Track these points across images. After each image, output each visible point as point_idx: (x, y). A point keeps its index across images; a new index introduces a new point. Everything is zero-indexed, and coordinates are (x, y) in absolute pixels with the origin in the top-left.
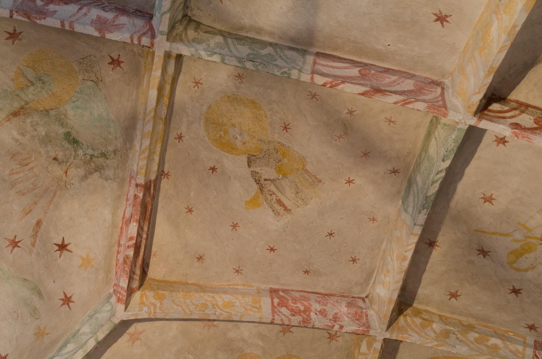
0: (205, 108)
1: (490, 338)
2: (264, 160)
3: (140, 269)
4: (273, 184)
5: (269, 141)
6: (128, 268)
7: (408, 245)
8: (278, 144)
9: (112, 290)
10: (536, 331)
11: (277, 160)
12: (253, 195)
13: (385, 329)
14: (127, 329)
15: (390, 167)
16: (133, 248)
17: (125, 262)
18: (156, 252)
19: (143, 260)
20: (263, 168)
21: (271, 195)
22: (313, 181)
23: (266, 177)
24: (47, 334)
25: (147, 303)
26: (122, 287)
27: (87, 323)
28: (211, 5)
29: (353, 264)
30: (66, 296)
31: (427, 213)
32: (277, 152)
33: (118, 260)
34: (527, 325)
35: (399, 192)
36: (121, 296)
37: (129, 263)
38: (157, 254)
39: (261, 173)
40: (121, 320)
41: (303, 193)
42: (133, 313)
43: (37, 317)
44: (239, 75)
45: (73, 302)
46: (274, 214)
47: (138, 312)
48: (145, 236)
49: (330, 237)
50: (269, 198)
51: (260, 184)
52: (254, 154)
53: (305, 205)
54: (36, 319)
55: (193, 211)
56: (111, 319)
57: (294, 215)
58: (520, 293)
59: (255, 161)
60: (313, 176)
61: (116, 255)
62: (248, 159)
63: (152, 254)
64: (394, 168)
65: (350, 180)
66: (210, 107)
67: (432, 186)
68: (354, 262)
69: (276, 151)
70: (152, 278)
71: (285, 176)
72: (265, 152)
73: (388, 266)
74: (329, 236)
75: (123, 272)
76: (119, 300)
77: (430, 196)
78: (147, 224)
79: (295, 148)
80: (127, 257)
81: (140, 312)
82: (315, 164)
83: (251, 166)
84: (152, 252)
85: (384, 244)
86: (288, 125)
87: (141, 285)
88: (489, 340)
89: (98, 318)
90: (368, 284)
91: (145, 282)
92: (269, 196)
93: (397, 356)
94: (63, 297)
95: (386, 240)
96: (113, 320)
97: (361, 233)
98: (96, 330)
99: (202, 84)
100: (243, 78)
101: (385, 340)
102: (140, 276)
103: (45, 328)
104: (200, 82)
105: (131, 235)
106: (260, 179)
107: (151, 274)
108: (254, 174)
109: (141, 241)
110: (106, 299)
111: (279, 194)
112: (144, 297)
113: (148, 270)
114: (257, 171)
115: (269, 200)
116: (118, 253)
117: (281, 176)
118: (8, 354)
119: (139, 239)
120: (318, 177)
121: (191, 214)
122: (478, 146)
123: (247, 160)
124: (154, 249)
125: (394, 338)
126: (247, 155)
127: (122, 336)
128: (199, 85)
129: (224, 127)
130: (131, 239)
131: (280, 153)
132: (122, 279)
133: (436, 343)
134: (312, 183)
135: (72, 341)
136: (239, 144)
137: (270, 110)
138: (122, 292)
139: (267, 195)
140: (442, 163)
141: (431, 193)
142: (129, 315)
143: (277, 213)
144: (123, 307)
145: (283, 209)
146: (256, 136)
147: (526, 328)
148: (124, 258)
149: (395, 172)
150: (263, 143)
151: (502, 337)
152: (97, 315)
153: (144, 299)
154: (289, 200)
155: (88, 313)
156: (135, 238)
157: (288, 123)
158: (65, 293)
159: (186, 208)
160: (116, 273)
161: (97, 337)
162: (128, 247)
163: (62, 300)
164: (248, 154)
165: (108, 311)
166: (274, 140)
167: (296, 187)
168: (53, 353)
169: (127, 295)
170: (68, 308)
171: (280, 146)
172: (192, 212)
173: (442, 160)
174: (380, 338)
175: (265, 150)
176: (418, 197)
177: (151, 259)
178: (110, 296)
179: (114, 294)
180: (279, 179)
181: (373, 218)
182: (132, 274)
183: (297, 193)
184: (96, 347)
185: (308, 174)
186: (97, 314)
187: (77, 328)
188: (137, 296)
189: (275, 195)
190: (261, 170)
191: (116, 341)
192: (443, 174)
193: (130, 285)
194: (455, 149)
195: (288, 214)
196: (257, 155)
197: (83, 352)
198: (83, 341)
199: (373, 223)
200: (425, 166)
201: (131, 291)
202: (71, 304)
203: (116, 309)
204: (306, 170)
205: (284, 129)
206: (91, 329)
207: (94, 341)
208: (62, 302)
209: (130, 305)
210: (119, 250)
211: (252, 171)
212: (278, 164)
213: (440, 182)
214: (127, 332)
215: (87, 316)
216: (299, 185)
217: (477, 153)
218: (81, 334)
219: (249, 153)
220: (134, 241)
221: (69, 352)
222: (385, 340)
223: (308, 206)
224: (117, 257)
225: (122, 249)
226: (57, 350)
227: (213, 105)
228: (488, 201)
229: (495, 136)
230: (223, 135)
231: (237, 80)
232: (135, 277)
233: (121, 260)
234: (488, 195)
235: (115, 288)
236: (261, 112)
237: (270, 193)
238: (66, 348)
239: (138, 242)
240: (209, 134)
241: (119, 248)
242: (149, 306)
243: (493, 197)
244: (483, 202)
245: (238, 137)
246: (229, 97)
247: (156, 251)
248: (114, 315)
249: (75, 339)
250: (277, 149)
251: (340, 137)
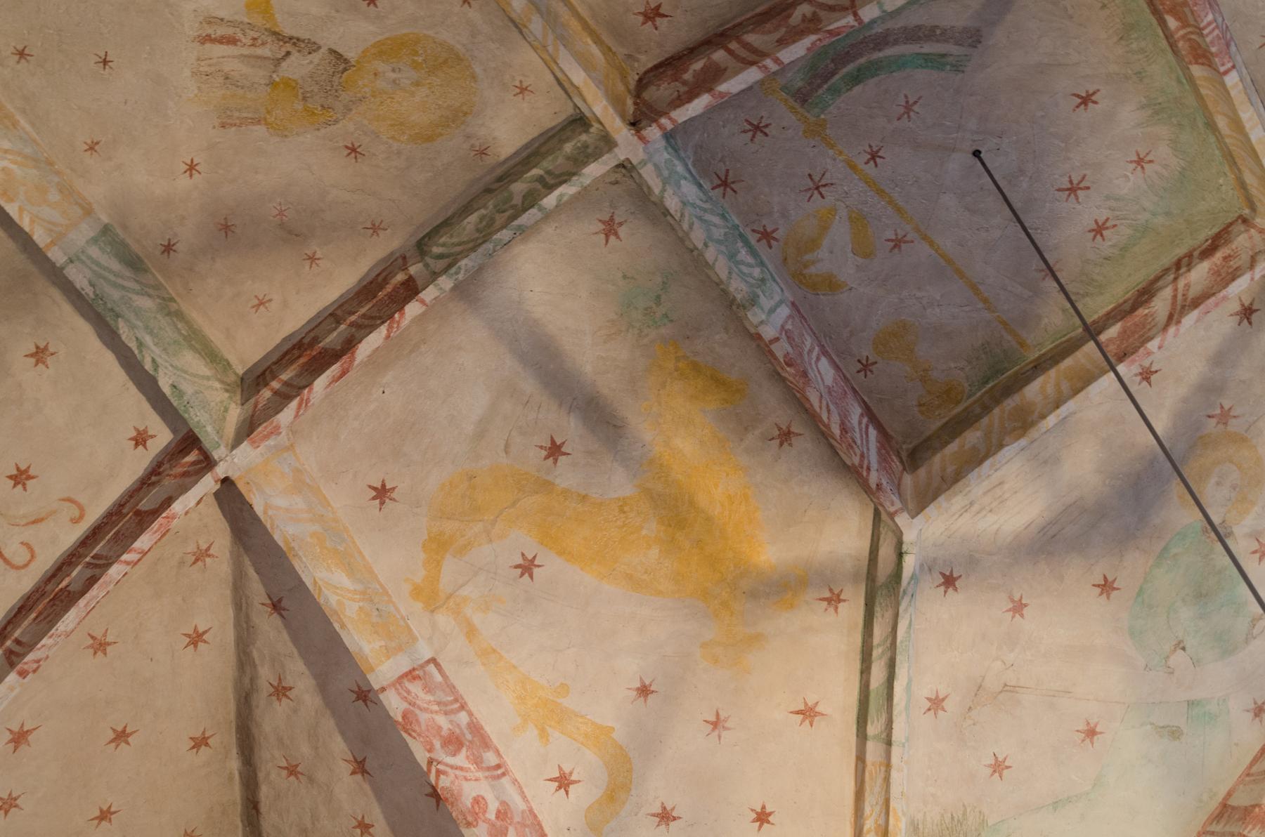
0: (478, 70)
2: (323, 77)
4: (272, 57)
5: (350, 110)
7: (32, 221)
8: (335, 118)
11: (308, 95)
12: (276, 16)
15: (179, 247)
20: (312, 66)
21: (254, 39)
22: (229, 117)
23: (292, 58)
28: (608, 204)
29: (15, 48)
31: (83, 293)
32: (322, 106)
35: (125, 227)
41: (219, 85)
44: (484, 153)
46: (214, 15)
49: (100, 57)
50: (252, 33)
51: (287, 39)
52: (345, 73)
53: (194, 70)
57: (187, 41)
59: (334, 65)
60: (241, 124)
62: (346, 60)
64: (174, 251)
65: (194, 172)
66: (474, 77)
67: (135, 339)
71: (272, 84)
72: (336, 91)
74: (104, 57)
77: (116, 322)
79: (309, 136)
82: (261, 143)
85: (28, 128)
86: (356, 158)
92: (255, 36)
95: (34, 135)
97: (75, 107)
99: (515, 95)
100: (476, 154)
104: (521, 95)
106: (297, 48)
108: (313, 47)
111: (246, 51)
114: (314, 54)
115: (247, 31)
117: (277, 79)
120: (233, 129)
122: (149, 400)
123: (346, 57)
126: (353, 63)
128: (518, 91)
129: (427, 70)
131: (317, 109)
134: (228, 113)
136: (381, 66)
137: (399, 153)
139: (258, 34)
140: (170, 382)
141: (120, 326)
143: (212, 20)
145: (213, 36)
146: (373, 99)
149: (168, 248)
150: (354, 99)
154: (223, 57)
157: (359, 160)
164: (354, 66)
166: (347, 119)
167: (239, 84)
171: (330, 119)
173: (175, 384)
176: (115, 285)
180: (274, 72)
183: (227, 78)
185: (250, 121)
189: (249, 44)
190: (311, 62)
192: (148, 366)
194: (186, 416)
195: (196, 34)
196: (341, 77)
199: (85, 143)
200: (167, 329)
204: (259, 122)
205: (353, 145)
211: (319, 48)
212: (301, 91)
213: (136, 352)
216: (240, 92)
217: (136, 390)
219: (354, 68)
223: (187, 73)
227: (473, 84)
228: (37, 352)
229: (155, 436)
230: (416, 58)
231: (480, 146)
234: (49, 360)
236: (405, 138)
237: (260, 42)
240: (435, 42)
243: (41, 366)
244: (39, 345)
245: (393, 75)
246: (465, 114)
250: (327, 111)
251: (281, 213)
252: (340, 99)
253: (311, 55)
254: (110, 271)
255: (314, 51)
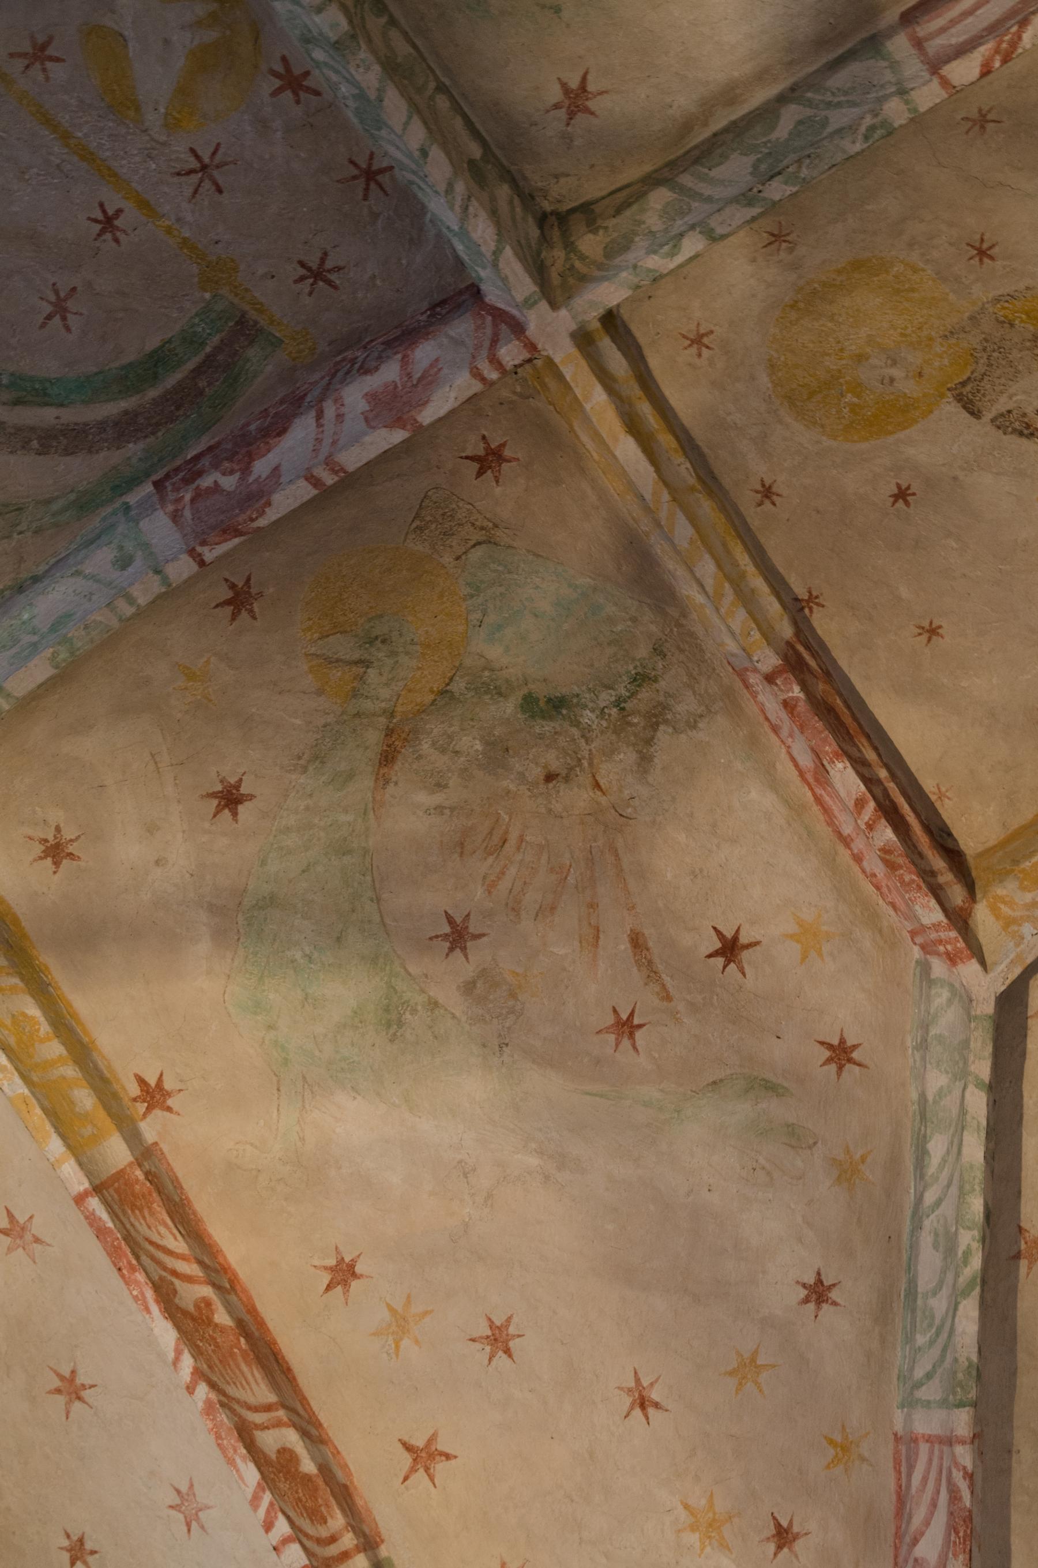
0: (764, 380)
2: (999, 372)
3: (937, 855)
5: (972, 318)
6: (910, 873)
8: (999, 306)
9: (916, 949)
11: (1028, 344)
14: (1026, 1007)
16: (883, 821)
17: (891, 866)
18: (939, 789)
19: (927, 829)
20: (1011, 391)
24: (863, 1159)
25: (1018, 914)
26: (934, 925)
27: (928, 1066)
28: (576, 143)
30: (830, 1047)
32: (1012, 325)
33: (874, 875)
36: (949, 947)
37: (900, 861)
38: (943, 789)
39: (1015, 405)
40: (996, 998)
42: (1008, 960)
43: (811, 1141)
44: (773, 235)
45: (855, 1047)
47: (1018, 950)
48: (883, 774)
52: (965, 377)
54: (810, 1148)
55: (940, 627)
56: (973, 1013)
59: (978, 391)
61: (856, 868)
62: (959, 401)
63: (933, 798)
66: (772, 367)
69: (1006, 325)
70: (980, 850)
72: (984, 350)
75: (907, 892)
76: (952, 959)
78: (866, 744)
80: (886, 851)
81: (1022, 946)
83: (979, 411)
84: (931, 796)
86: (982, 240)
87: (970, 887)
89: (940, 1035)
91: (974, 874)
94: (827, 1054)
96: (978, 1012)
98: (961, 1065)
99: (712, 332)
100: (788, 234)
102: (951, 869)
103: (847, 1151)
104: (702, 331)
105: (854, 797)
106: (1026, 420)
107: (972, 844)
108: (1002, 422)
109: (885, 791)
110: (921, 981)
112: (1002, 906)
113: (955, 840)
114: (1003, 410)
116: (858, 859)
118: (819, 1269)
119: (878, 791)
121: (942, 637)
123: (959, 405)
124: (928, 785)
126: (949, 394)
127: (1029, 1033)
128: (705, 340)
129: (841, 380)
130: (860, 804)
131: (1022, 321)
132: (917, 907)
135: (928, 1132)
136: (909, 388)
137: (911, 245)
138: (943, 935)
142: (1002, 971)
144: (974, 965)
146: (933, 333)
148: (882, 859)
150: (962, 335)
152: (933, 1031)
153: (1005, 909)
155: (909, 1042)
156: (868, 795)
157: (978, 237)
158: (822, 1043)
159: (920, 634)
160: (893, 905)
161: (977, 1077)
162: (870, 827)
163: (829, 1061)
164: (949, 389)
165: (950, 1002)
166: (980, 304)
168: (912, 1191)
169: (960, 934)
170: (857, 1069)
171: (1006, 305)
172: (940, 631)
175: (979, 347)
177: (941, 811)
178: (925, 968)
179: (928, 956)
182: (929, 879)
184: (991, 1103)
186: (930, 1027)
187: (914, 1096)
188: (982, 916)
190: (1010, 398)
191: (1023, 1055)
193: (947, 905)
196: (972, 373)
197: (976, 1134)
198: (955, 1111)
201: (960, 916)
202: (855, 1055)
203: (965, 984)
205: (981, 260)
206: (947, 1072)
207: (976, 1091)
208: (833, 1067)
209: (984, 948)
210: (856, 851)
211: (992, 421)
214: (1030, 1013)
215: (913, 1053)
218: (935, 1102)
219: (949, 385)
220: (872, 804)
221: (944, 1160)
224: (864, 871)
225: (859, 844)
226: (913, 1177)
227: (775, 355)
230: (855, 400)
231: (779, 250)
232: (941, 879)
233: (879, 869)
235: (919, 940)
236: (896, 269)
238: (930, 1157)
239: (882, 799)
240: (822, 426)
241: (850, 849)
242: (1028, 917)
245: (895, 372)
246: (793, 306)
247: (938, 785)
248: (971, 1001)
249: (933, 1123)
250: (1006, 317)
252: (983, 336)
253: (1009, 408)
255: (1002, 415)
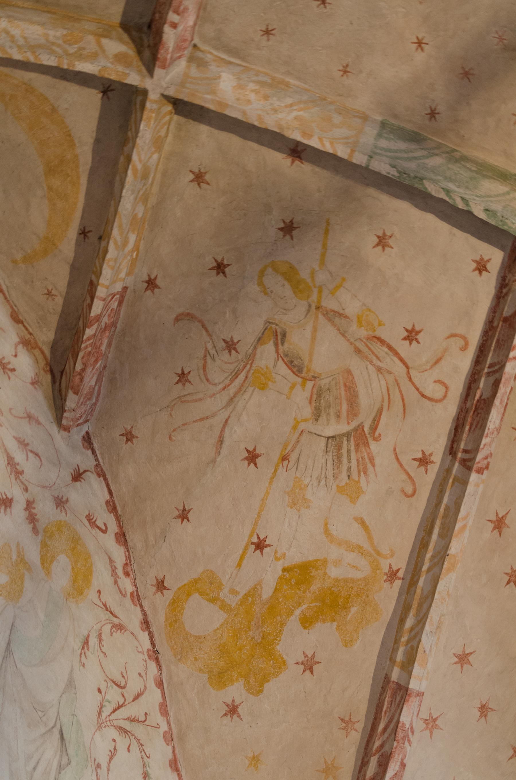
1: (136, 233)
7: (332, 143)
10: (146, 290)
13: (166, 93)
15: (441, 108)
29: (261, 30)
31: (390, 176)
34: (156, 278)
35: (395, 116)
58: (218, 274)
64: (438, 113)
65: (423, 45)
67: (442, 189)
68: (264, 31)
73: (275, 98)
77: (422, 184)
85: (297, 83)
88: (134, 233)
90: (217, 49)
93: (73, 84)
95: (306, 86)
97: (320, 49)
101: (145, 93)
122: (473, 235)
125: (148, 105)
133: (139, 166)
140: (482, 208)
141: (427, 186)
147: (149, 276)
149: (433, 114)
151: (136, 248)
173: (487, 208)
174: (148, 84)
176: (409, 159)
181: (349, 72)
192: (461, 205)
194: (505, 228)
199: (340, 70)
200: (461, 172)
213: (447, 199)
217: (461, 232)
222: (145, 93)
228: (380, 241)
229: (490, 259)
234: (391, 242)
243: (387, 249)
244: (378, 234)
251: (501, 38)
254: (401, 151)
